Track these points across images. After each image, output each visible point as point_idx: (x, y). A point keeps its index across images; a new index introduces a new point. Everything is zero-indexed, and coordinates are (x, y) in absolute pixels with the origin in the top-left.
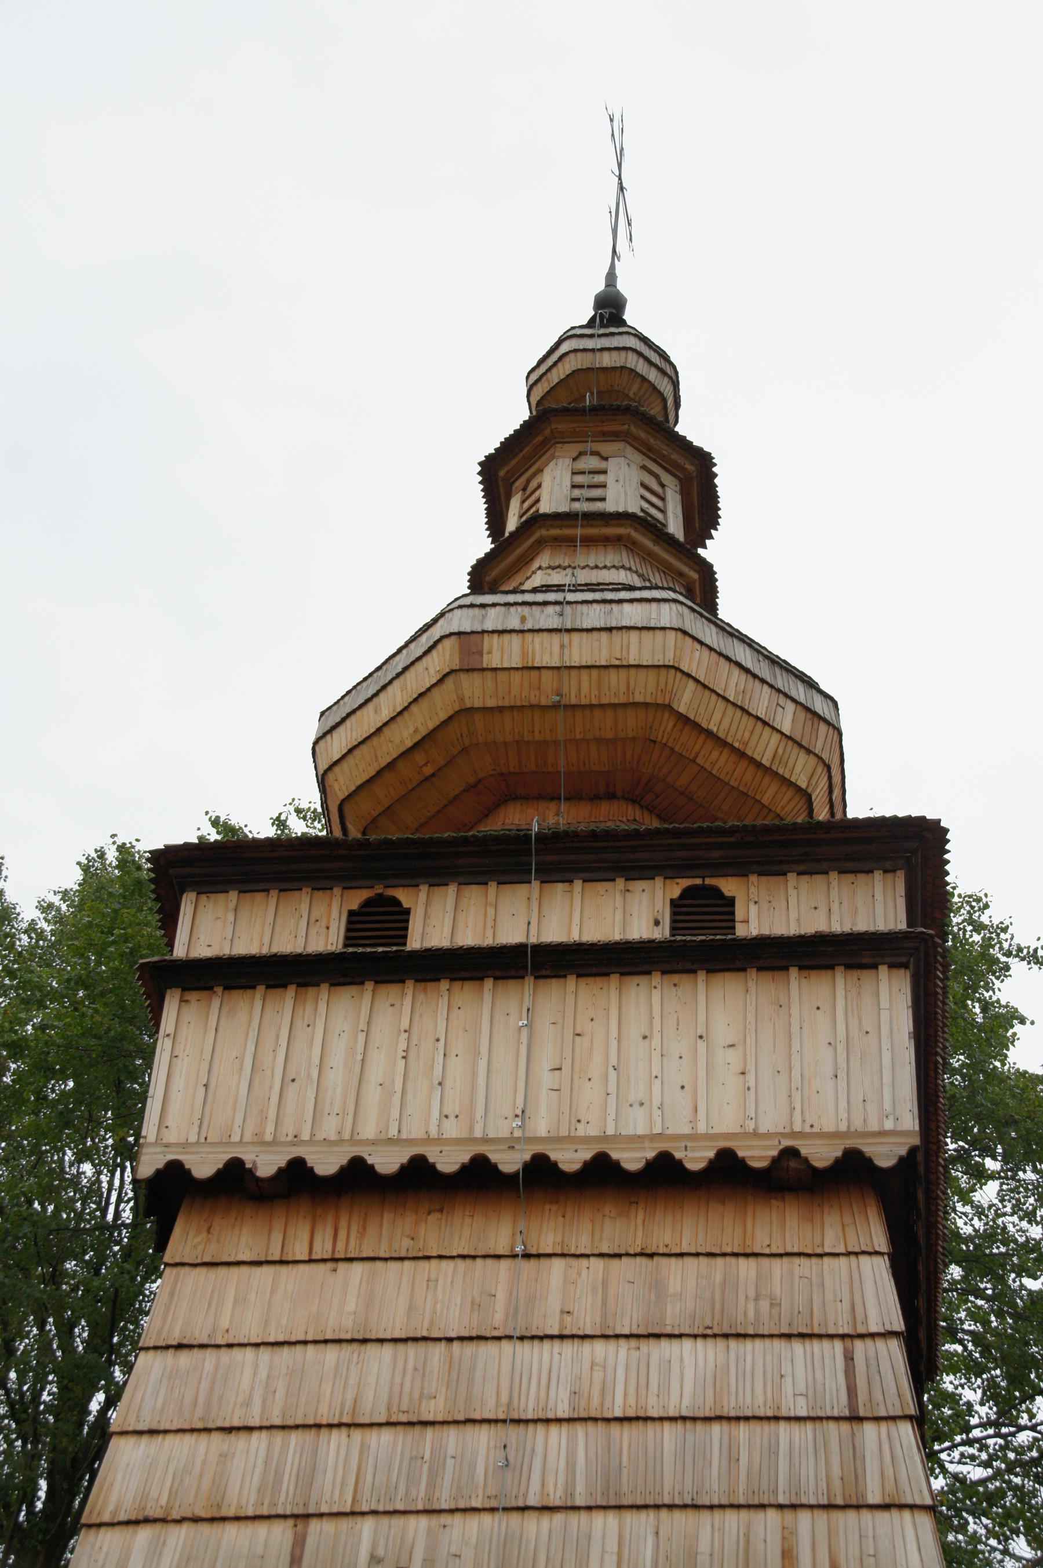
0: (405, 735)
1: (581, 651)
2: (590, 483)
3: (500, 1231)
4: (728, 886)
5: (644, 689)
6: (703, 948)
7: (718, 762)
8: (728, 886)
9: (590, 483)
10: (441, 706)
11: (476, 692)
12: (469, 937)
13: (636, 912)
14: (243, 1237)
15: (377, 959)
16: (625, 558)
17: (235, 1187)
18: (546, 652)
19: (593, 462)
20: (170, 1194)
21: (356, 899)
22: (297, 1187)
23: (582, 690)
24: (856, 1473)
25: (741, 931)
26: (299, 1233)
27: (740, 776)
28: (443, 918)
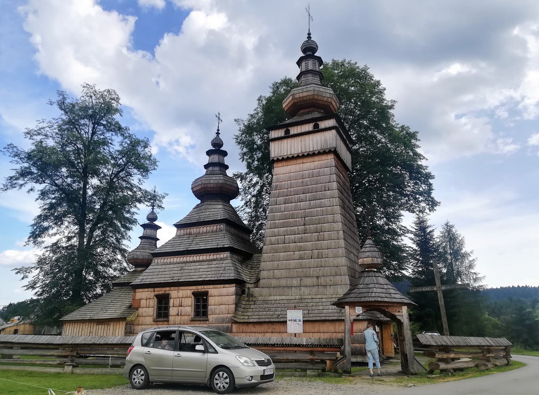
0: (290, 105)
1: (305, 94)
2: (307, 65)
3: (300, 161)
4: (318, 123)
5: (311, 97)
6: (317, 130)
7: (321, 102)
8: (318, 123)
9: (307, 65)
10: (292, 102)
11: (295, 101)
12: (296, 132)
13: (309, 127)
14: (280, 164)
15: (288, 136)
16: (311, 75)
17: (278, 160)
18: (301, 95)
19: (307, 62)
20: (273, 161)
21: (285, 129)
22: (283, 160)
23: (305, 98)
24: (330, 180)
25: (320, 128)
26: (284, 163)
27: (323, 103)
28: (294, 130)
